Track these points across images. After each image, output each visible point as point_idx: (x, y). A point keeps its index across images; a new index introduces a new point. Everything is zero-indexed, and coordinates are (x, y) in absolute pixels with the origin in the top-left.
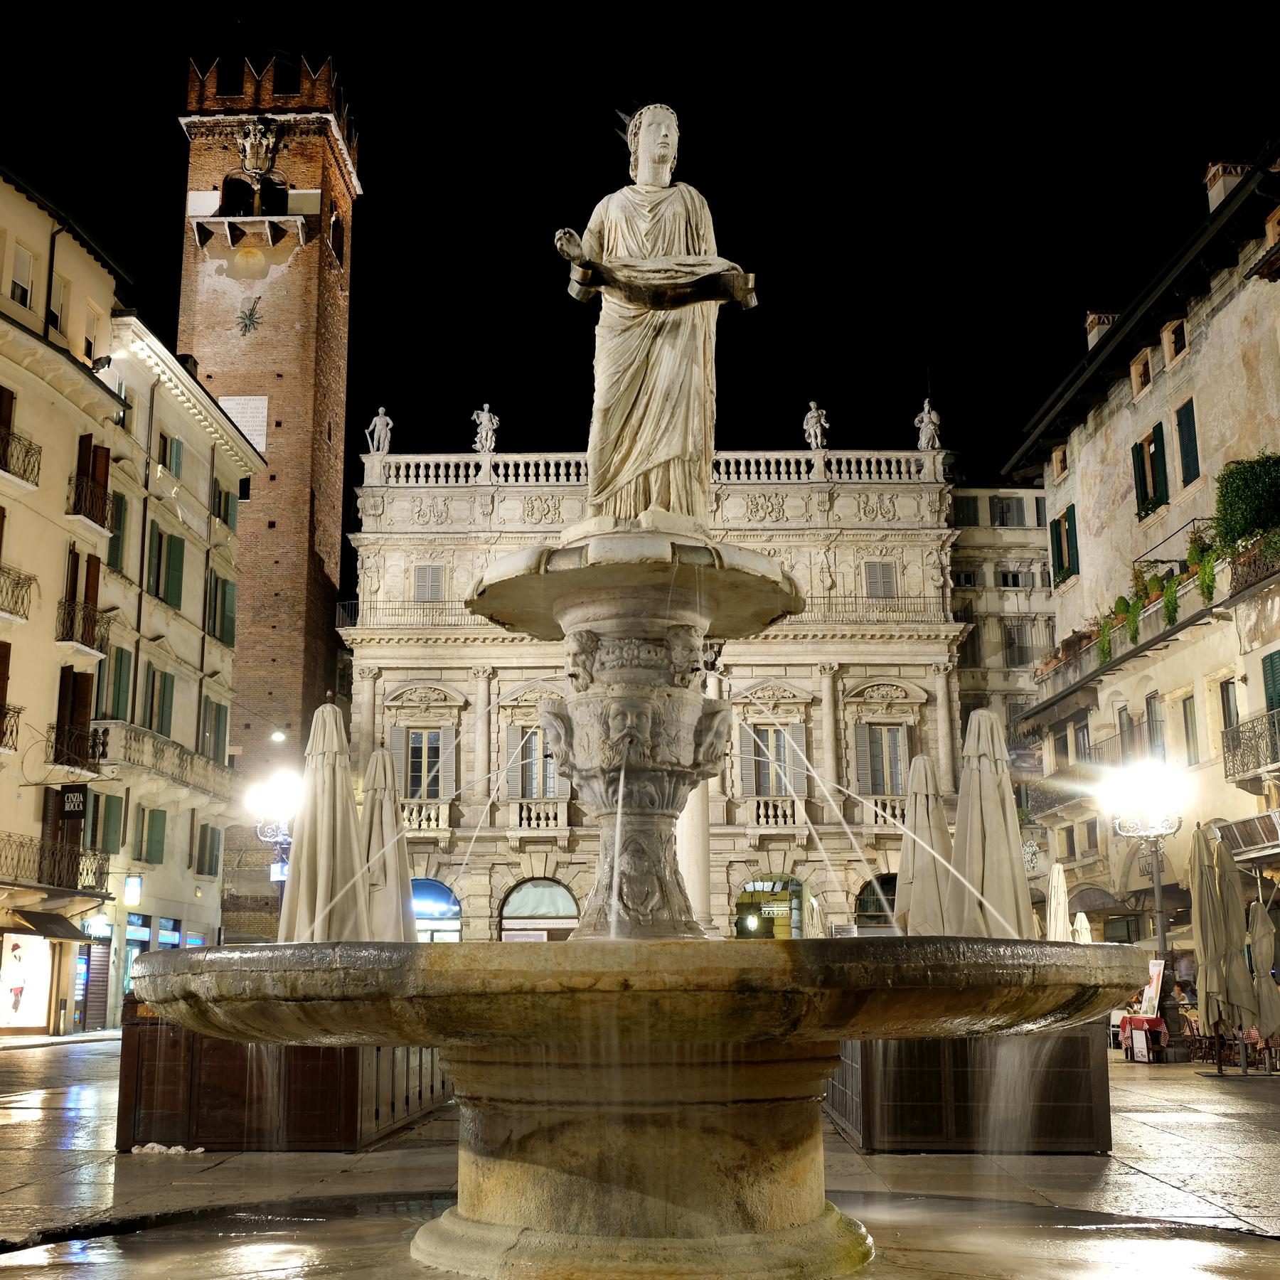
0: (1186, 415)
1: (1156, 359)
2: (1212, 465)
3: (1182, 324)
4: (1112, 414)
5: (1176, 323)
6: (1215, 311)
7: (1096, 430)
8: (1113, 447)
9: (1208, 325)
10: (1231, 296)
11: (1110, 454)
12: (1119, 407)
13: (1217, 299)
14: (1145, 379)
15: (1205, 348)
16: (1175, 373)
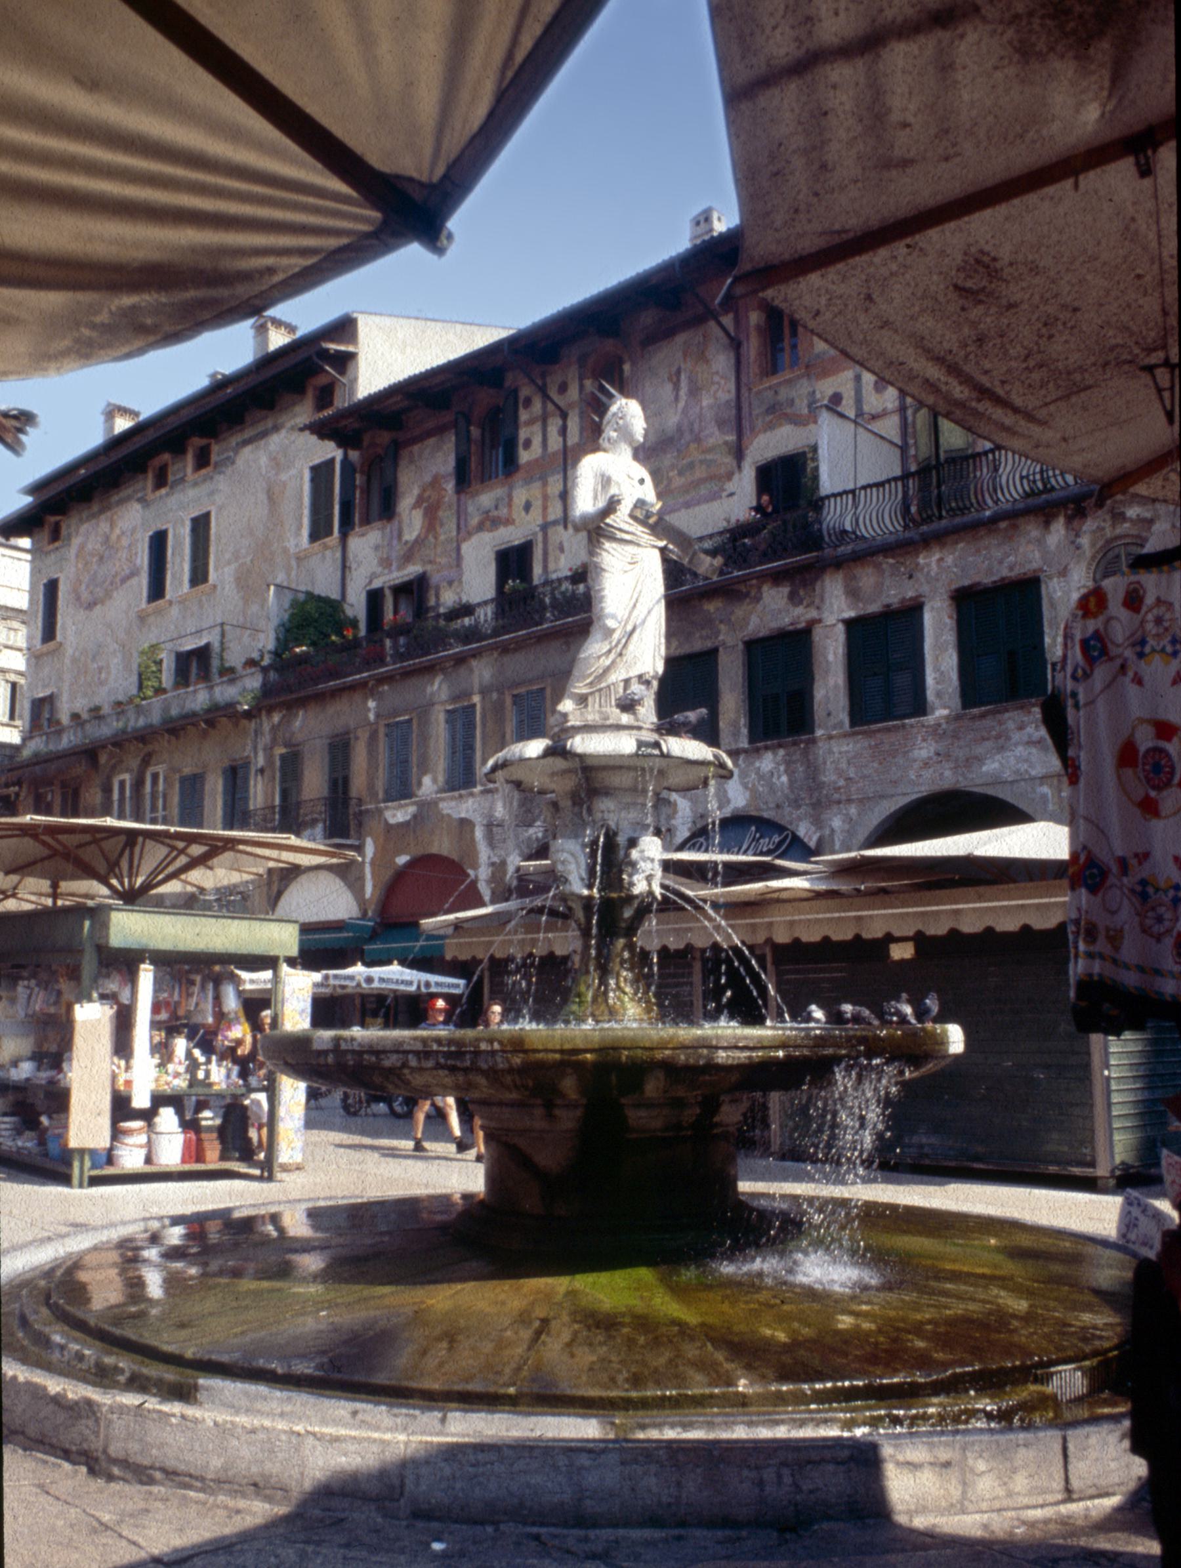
0: (201, 525)
1: (176, 467)
2: (219, 572)
3: (209, 445)
4: (121, 502)
5: (204, 442)
6: (246, 442)
7: (102, 511)
8: (117, 531)
9: (236, 453)
10: (264, 434)
11: (114, 537)
12: (128, 499)
13: (248, 433)
14: (161, 481)
15: (229, 471)
16: (196, 484)
